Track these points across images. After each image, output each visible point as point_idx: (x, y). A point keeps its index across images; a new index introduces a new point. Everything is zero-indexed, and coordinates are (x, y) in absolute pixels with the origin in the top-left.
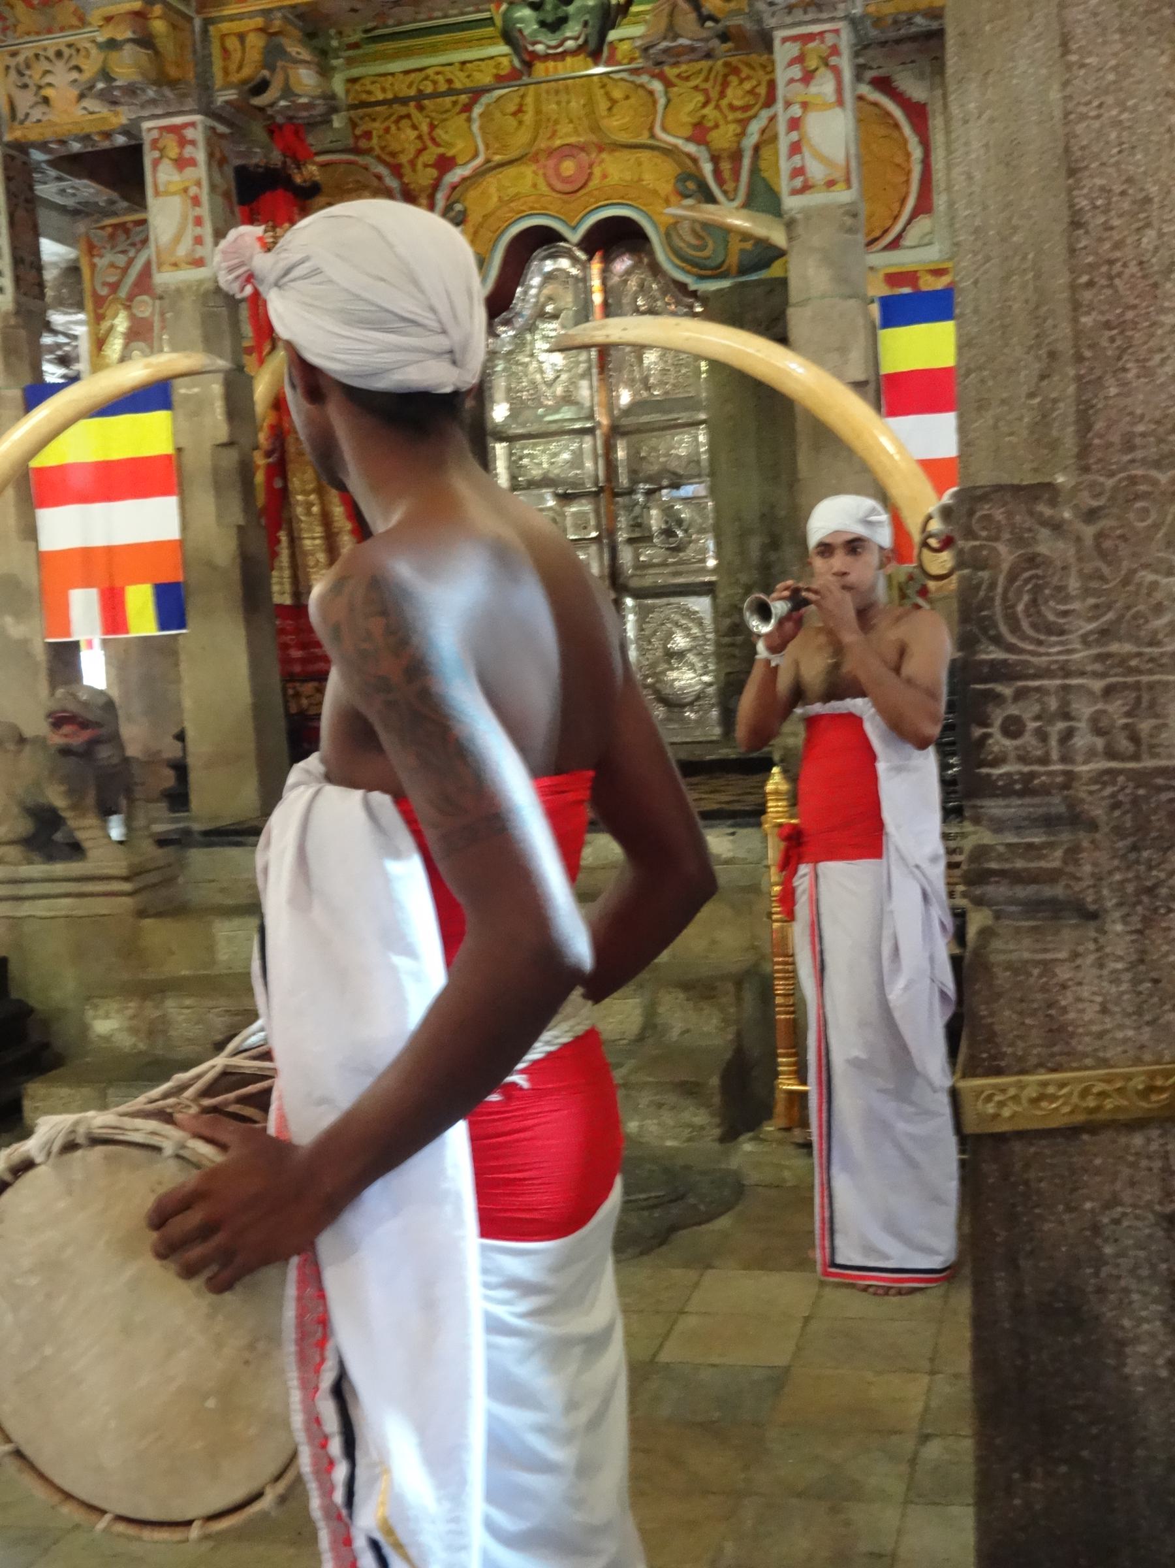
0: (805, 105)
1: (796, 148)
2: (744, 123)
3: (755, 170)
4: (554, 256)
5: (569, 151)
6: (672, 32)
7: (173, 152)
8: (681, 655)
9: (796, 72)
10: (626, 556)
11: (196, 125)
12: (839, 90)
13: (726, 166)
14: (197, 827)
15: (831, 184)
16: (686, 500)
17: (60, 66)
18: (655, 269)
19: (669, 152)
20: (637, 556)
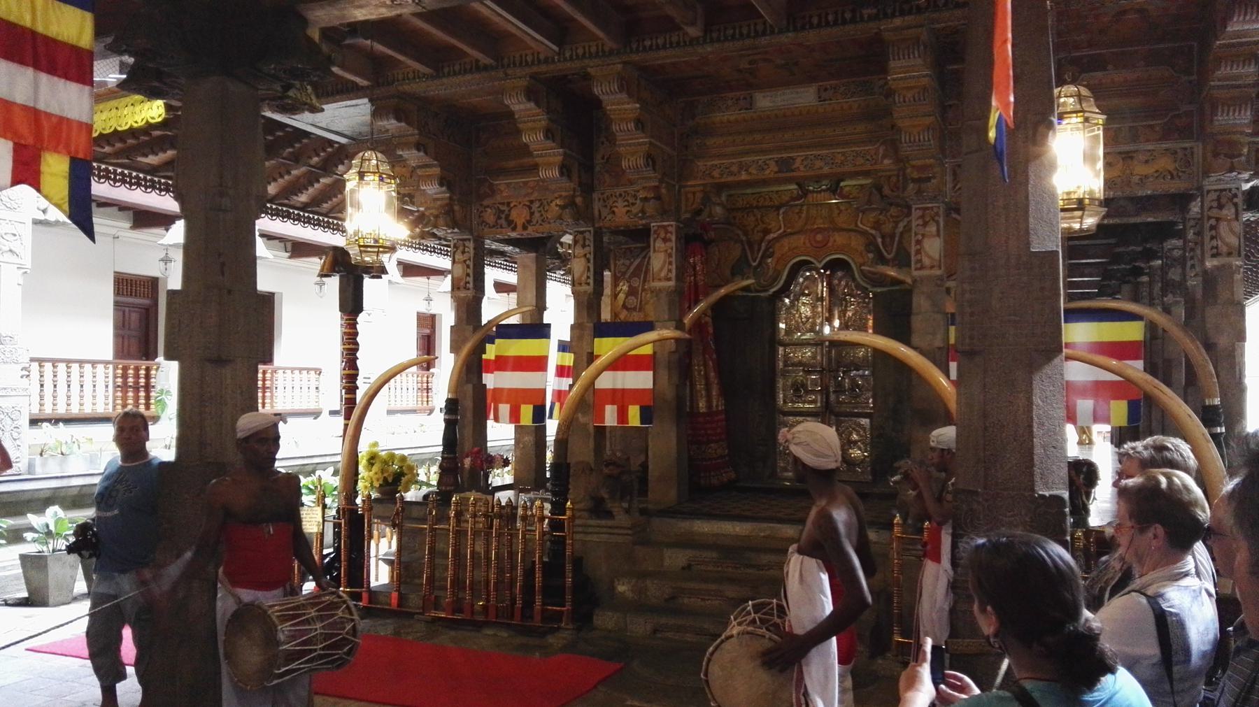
0: (923, 235)
1: (918, 252)
2: (897, 223)
3: (900, 242)
4: (809, 270)
5: (820, 230)
6: (869, 202)
7: (662, 235)
8: (855, 442)
9: (920, 222)
10: (832, 397)
11: (671, 224)
12: (938, 230)
13: (888, 240)
14: (650, 506)
15: (932, 267)
16: (862, 377)
17: (620, 200)
18: (854, 280)
19: (864, 233)
20: (838, 398)
